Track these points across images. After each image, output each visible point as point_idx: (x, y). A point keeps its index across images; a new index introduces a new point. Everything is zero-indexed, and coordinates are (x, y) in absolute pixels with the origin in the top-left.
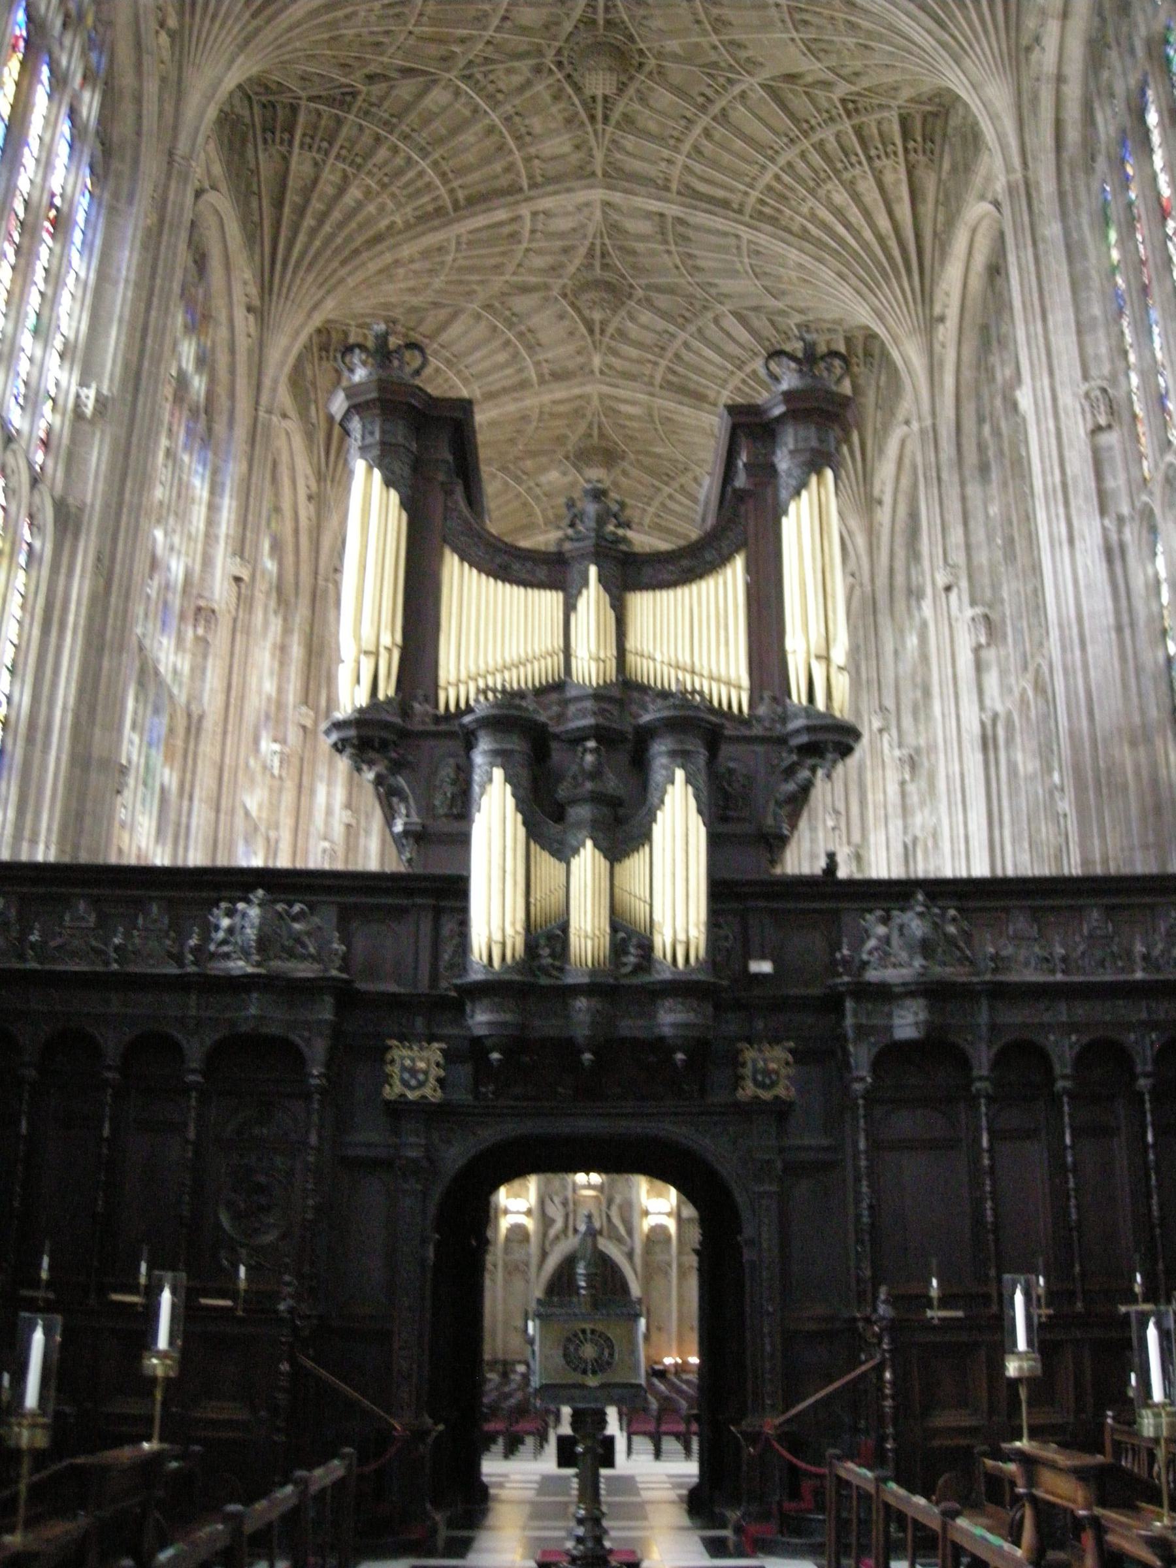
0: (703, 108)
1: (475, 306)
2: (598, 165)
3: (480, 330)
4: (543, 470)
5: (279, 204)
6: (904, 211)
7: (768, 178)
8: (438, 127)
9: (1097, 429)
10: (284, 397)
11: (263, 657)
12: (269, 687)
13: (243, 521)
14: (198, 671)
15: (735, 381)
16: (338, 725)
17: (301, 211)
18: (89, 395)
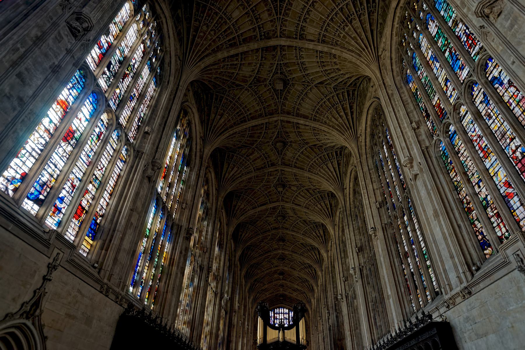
6: (318, 256)
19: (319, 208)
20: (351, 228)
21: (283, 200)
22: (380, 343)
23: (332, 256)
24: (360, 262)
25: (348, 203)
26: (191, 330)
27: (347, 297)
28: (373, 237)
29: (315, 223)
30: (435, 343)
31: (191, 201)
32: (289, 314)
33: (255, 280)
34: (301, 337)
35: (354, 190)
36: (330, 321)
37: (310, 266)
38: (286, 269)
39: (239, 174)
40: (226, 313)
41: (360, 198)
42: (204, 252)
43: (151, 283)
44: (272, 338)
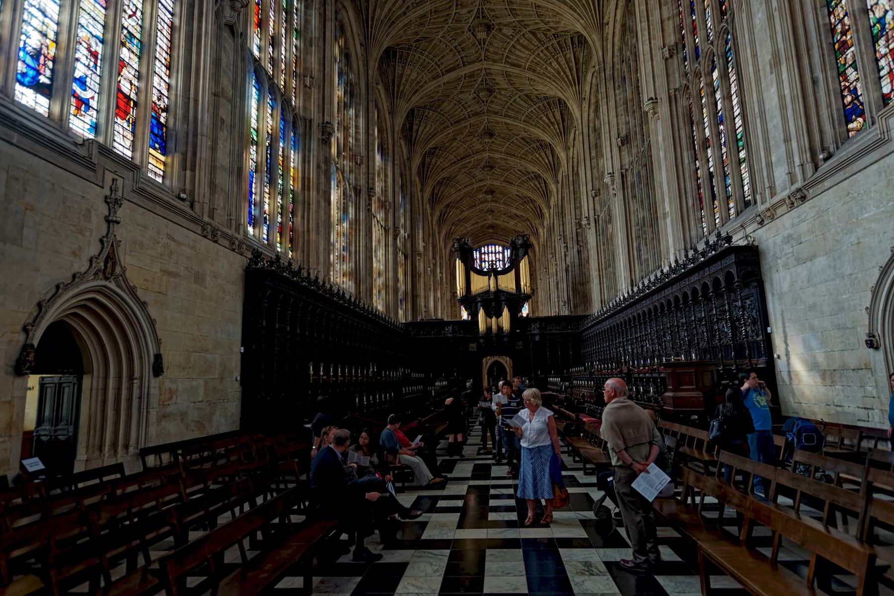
5: (423, 167)
6: (551, 158)
17: (428, 168)
19: (554, 69)
20: (612, 103)
21: (487, 58)
22: (643, 283)
23: (575, 156)
24: (624, 163)
25: (610, 53)
26: (356, 283)
27: (596, 221)
28: (650, 115)
29: (546, 98)
30: (729, 276)
31: (319, 70)
32: (503, 253)
33: (448, 206)
34: (522, 283)
35: (623, 25)
36: (568, 259)
37: (537, 177)
38: (497, 183)
39: (400, 8)
40: (406, 257)
41: (634, 41)
42: (356, 163)
43: (279, 220)
44: (479, 287)
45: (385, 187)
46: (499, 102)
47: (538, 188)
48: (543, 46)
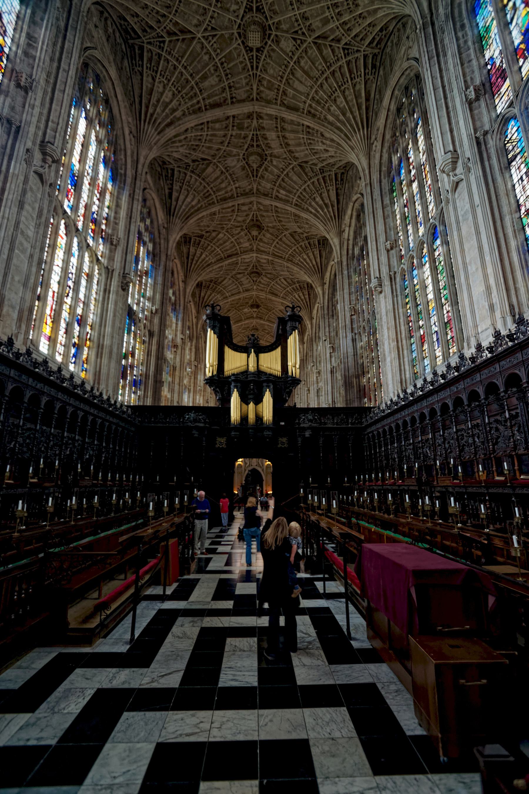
0: (277, 238)
1: (229, 277)
2: (255, 248)
3: (230, 282)
4: (243, 309)
5: (188, 258)
7: (290, 252)
8: (221, 242)
9: (352, 315)
10: (190, 299)
11: (187, 351)
12: (188, 357)
13: (183, 327)
14: (175, 358)
15: (284, 292)
16: (206, 380)
17: (193, 260)
18: (154, 308)
27: (392, 279)
34: (290, 364)
38: (263, 295)
40: (151, 334)
45: (115, 218)
46: (271, 177)
47: (302, 300)
48: (309, 180)
